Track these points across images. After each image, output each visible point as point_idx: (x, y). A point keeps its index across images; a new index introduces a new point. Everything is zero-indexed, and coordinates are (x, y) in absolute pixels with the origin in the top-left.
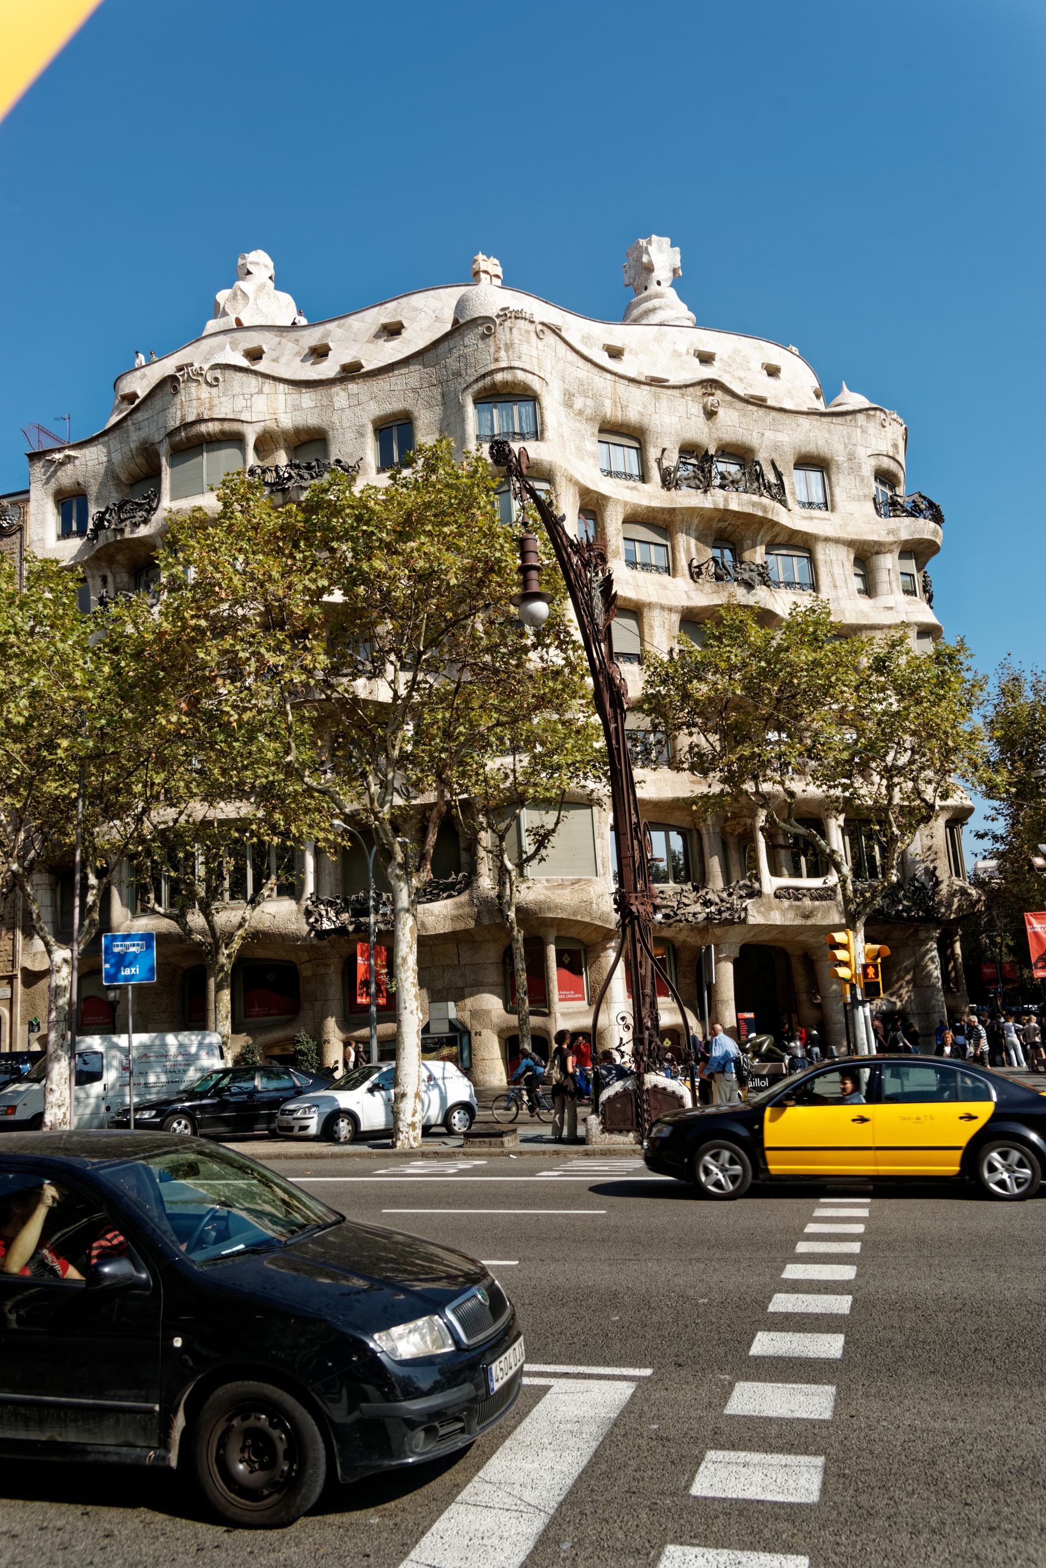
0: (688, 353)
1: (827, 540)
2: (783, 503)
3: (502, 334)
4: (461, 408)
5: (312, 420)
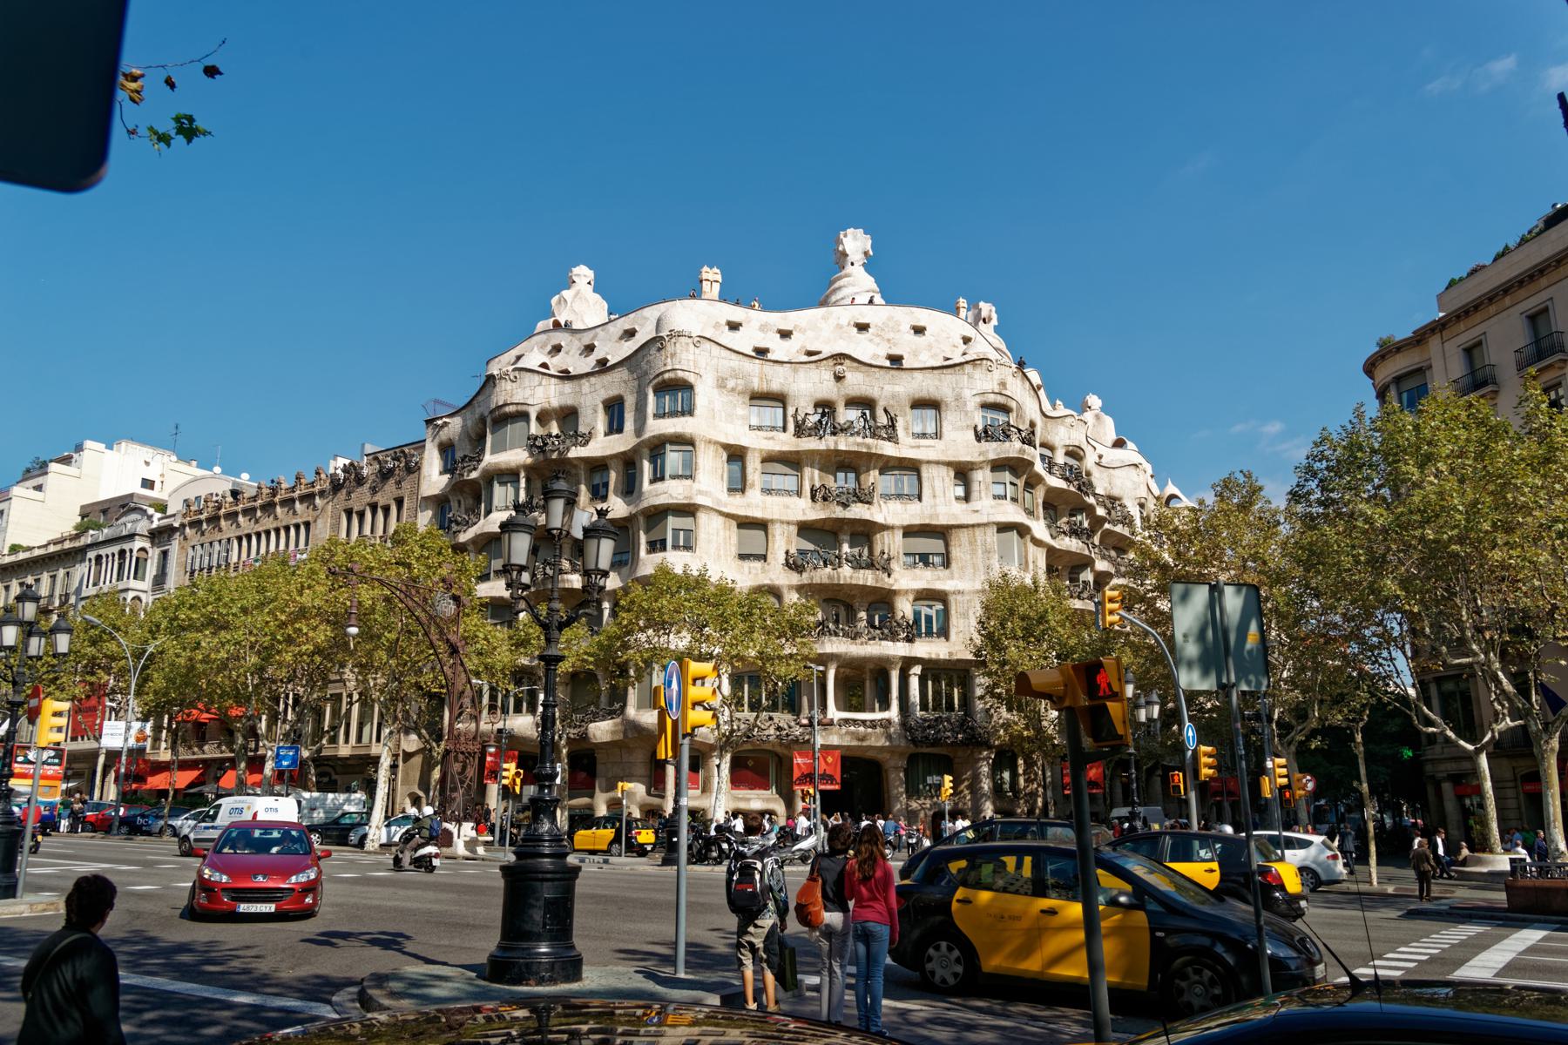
1: (929, 462)
2: (892, 438)
3: (670, 348)
4: (646, 395)
5: (570, 402)
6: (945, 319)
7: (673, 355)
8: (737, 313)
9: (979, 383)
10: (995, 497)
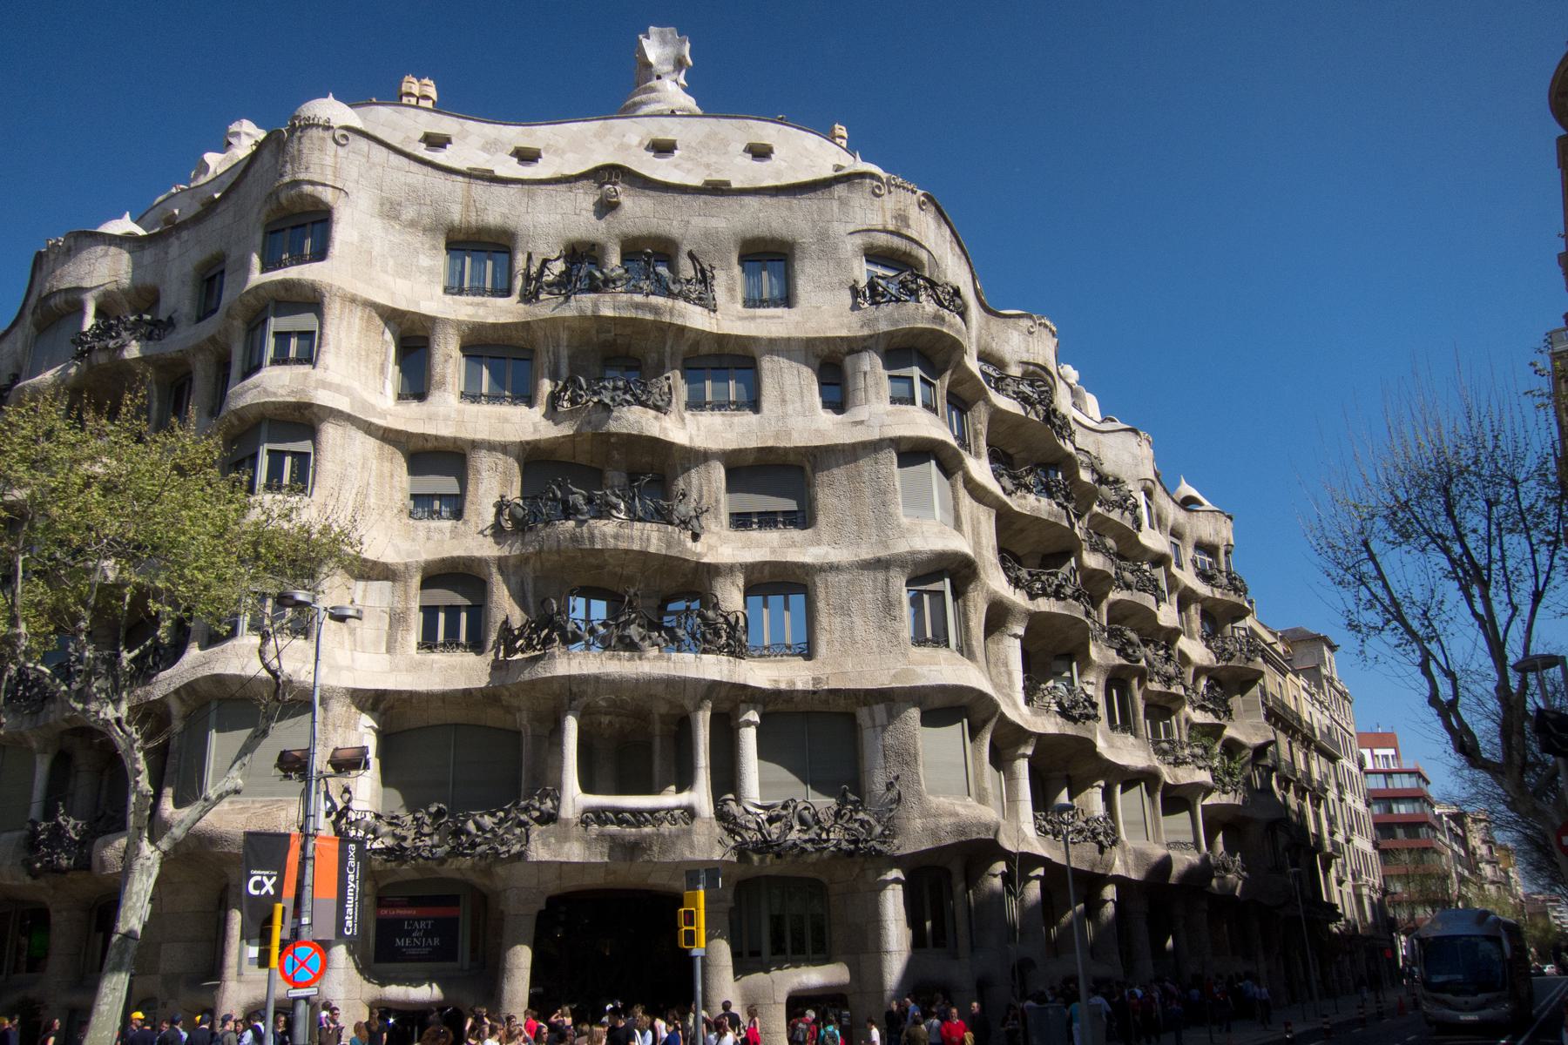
0: (641, 144)
6: (811, 141)
7: (296, 159)
8: (444, 124)
9: (859, 214)
10: (894, 401)
